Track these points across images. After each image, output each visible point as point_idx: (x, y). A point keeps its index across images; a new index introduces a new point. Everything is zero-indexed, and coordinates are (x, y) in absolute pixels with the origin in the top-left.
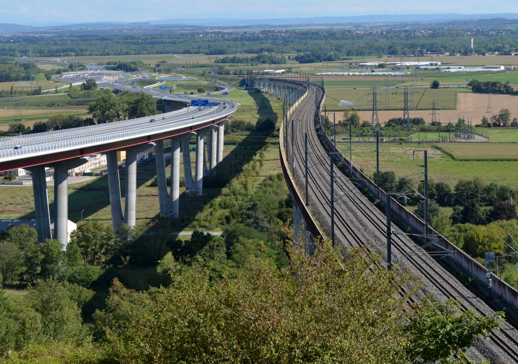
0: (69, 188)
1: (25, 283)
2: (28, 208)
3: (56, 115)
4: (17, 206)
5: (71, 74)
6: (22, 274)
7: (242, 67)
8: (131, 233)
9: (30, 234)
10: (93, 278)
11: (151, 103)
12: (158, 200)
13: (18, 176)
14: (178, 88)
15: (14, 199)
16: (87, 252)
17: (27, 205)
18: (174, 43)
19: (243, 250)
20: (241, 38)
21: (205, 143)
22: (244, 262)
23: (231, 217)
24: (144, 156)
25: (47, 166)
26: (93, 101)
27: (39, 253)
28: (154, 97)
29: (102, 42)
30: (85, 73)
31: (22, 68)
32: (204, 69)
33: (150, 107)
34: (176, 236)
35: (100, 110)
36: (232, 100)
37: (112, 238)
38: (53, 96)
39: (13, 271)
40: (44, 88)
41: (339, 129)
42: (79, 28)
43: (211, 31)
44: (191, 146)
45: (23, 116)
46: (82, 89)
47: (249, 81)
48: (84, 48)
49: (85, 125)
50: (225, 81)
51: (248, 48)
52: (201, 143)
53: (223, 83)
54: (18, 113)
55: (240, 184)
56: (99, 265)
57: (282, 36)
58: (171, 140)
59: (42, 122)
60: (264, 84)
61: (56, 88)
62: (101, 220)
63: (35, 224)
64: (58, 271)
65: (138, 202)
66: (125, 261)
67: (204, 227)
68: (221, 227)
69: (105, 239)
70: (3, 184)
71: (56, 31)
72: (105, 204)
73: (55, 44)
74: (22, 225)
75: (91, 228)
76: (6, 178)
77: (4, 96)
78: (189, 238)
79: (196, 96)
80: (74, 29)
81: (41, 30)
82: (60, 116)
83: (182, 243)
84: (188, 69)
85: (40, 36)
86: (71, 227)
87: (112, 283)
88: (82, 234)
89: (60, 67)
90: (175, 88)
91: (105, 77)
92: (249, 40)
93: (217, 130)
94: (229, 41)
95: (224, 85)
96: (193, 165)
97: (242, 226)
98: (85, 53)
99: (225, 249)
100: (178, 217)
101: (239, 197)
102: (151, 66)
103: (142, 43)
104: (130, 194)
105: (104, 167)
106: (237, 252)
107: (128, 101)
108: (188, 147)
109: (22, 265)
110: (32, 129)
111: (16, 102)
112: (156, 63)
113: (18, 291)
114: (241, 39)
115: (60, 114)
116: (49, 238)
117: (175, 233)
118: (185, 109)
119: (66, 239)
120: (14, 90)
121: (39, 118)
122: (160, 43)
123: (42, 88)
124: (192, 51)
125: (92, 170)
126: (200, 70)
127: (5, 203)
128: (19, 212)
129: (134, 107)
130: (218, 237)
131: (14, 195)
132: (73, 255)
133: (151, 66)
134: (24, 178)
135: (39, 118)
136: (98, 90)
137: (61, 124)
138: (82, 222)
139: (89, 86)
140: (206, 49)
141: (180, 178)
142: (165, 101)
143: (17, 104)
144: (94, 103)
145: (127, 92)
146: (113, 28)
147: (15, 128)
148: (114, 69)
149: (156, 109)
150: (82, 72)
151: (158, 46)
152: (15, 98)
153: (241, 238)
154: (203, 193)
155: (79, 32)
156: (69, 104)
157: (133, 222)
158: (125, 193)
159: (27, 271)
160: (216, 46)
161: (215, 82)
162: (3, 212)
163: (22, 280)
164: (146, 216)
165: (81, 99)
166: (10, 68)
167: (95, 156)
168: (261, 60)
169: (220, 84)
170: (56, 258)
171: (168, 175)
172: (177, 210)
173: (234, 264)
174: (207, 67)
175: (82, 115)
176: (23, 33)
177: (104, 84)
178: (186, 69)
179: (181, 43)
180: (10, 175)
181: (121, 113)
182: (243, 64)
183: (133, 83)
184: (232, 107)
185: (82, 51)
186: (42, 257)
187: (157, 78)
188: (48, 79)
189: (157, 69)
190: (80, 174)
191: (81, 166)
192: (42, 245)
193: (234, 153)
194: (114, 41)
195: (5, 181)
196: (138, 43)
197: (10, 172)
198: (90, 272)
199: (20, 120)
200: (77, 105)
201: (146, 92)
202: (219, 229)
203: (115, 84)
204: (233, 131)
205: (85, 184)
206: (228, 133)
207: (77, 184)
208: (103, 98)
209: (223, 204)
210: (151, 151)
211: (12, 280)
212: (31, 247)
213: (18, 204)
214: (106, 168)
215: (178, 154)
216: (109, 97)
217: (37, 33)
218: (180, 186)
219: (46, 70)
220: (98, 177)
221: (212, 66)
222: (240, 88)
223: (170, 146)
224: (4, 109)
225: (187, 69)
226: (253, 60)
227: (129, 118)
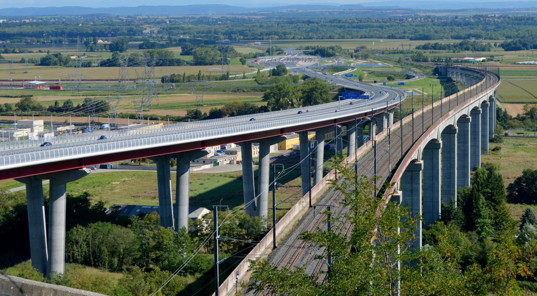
5: (267, 59)
7: (443, 54)
14: (370, 75)
18: (381, 27)
20: (451, 23)
29: (308, 25)
30: (280, 58)
38: (240, 82)
41: (516, 123)
42: (289, 10)
43: (424, 14)
47: (443, 70)
48: (288, 31)
50: (420, 69)
51: (456, 34)
53: (415, 70)
57: (494, 21)
60: (457, 73)
71: (266, 12)
73: (261, 26)
80: (285, 11)
81: (252, 12)
85: (249, 18)
92: (459, 25)
94: (438, 25)
95: (416, 73)
98: (288, 36)
103: (348, 27)
110: (208, 114)
111: (203, 87)
112: (355, 48)
114: (452, 24)
122: (367, 27)
124: (397, 36)
126: (397, 57)
133: (350, 51)
140: (412, 34)
146: (324, 11)
147: (193, 113)
148: (311, 54)
150: (278, 57)
151: (364, 30)
152: (201, 83)
155: (289, 14)
156: (254, 90)
160: (424, 30)
168: (464, 47)
176: (233, 14)
179: (389, 27)
182: (444, 51)
185: (285, 34)
189: (354, 54)
194: (320, 24)
196: (345, 26)
217: (246, 14)
221: (412, 52)
225: (385, 54)
226: (455, 46)
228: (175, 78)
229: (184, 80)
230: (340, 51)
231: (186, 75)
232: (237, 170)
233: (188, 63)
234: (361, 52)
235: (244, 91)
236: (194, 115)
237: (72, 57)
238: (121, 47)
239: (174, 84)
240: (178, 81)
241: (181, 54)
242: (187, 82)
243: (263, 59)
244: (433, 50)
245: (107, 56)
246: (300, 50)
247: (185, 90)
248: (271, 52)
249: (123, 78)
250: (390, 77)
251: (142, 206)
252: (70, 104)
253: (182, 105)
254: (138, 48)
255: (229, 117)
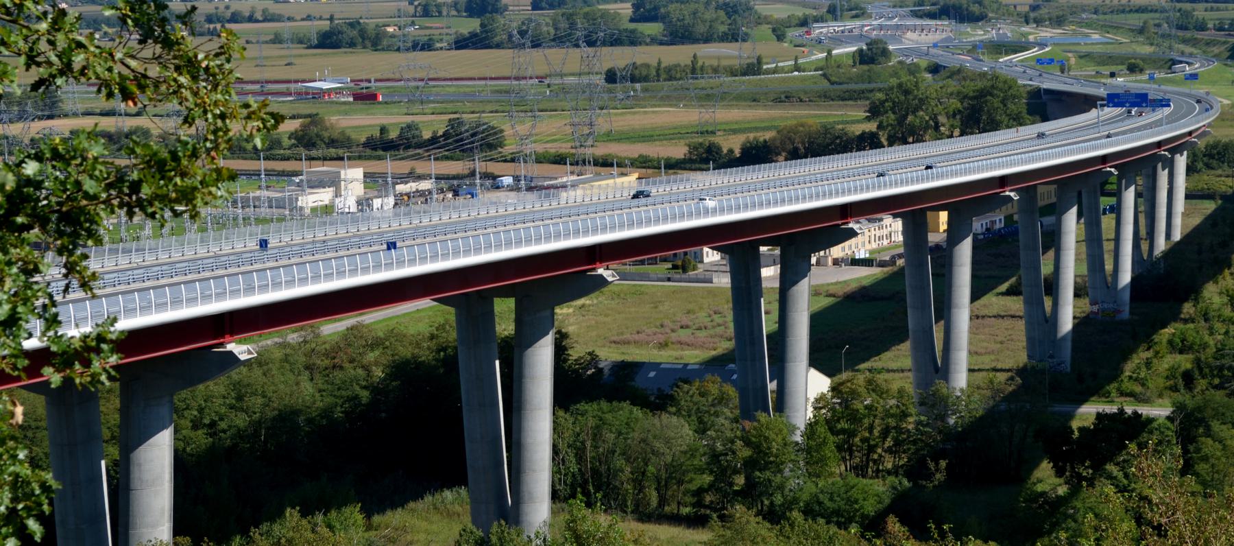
0: (815, 292)
1: (708, 512)
2: (721, 336)
3: (794, 122)
4: (699, 334)
6: (700, 492)
8: (954, 404)
9: (722, 400)
10: (862, 507)
11: (1014, 97)
12: (1023, 328)
13: (702, 262)
14: (1083, 61)
15: (692, 316)
16: (853, 445)
17: (720, 330)
19: (1219, 454)
21: (1138, 195)
22: (1222, 483)
23: (1197, 372)
24: (993, 223)
25: (765, 242)
26: (880, 90)
27: (739, 443)
28: (1020, 82)
30: (863, 26)
31: (722, 13)
32: (1145, 16)
33: (1011, 106)
34: (1071, 416)
35: (894, 113)
36: (1208, 93)
37: (911, 415)
39: (680, 482)
40: (769, 60)
44: (1105, 201)
45: (718, 124)
46: (854, 62)
49: (860, 148)
50: (1194, 45)
52: (1129, 196)
54: (707, 116)
55: (1221, 293)
56: (877, 477)
58: (1055, 186)
59: (761, 139)
61: (796, 59)
62: (888, 371)
63: (735, 377)
64: (781, 487)
65: (973, 331)
66: (937, 470)
67: (1131, 394)
68: (1171, 397)
69: (892, 416)
70: (669, 280)
72: (897, 335)
74: (709, 376)
75: (860, 390)
76: (675, 267)
77: (678, 76)
78: (1089, 422)
79: (1122, 82)
82: (802, 125)
83: (1072, 432)
84: (1107, 17)
86: (817, 384)
87: (885, 528)
88: (840, 404)
89: (808, 12)
90: (1073, 61)
91: (909, 35)
93: (1170, 165)
95: (1191, 55)
96: (1108, 246)
97: (1219, 396)
99: (1178, 450)
100: (1069, 370)
101: (1218, 326)
102: (1019, 8)
104: (955, 311)
105: (900, 246)
106: (1205, 459)
107: (959, 93)
108: (1097, 204)
109: (700, 471)
110: (737, 153)
111: (705, 92)
113: (691, 531)
115: (804, 120)
116: (766, 410)
117: (1058, 408)
118: (1094, 113)
119: (802, 413)
120: (700, 63)
121: (757, 129)
123: (764, 60)
125: (871, 252)
126: (1136, 20)
127: (671, 325)
128: (702, 347)
129: (973, 106)
130: (1161, 421)
131: (691, 306)
132: (817, 451)
133: (1019, 8)
134: (714, 268)
135: (757, 129)
136: (893, 66)
137: (803, 143)
138: (844, 376)
139: (872, 55)
141: (1076, 276)
142: (1048, 91)
143: (708, 95)
144: (880, 96)
145: (959, 71)
147: (701, 150)
149: (1025, 111)
150: (858, 23)
152: (702, 83)
153: (1216, 426)
154: (1131, 313)
156: (825, 97)
157: (960, 379)
158: (944, 309)
159: (711, 486)
161: (1170, 48)
162: (666, 345)
163: (699, 504)
164: (993, 365)
165: (852, 86)
166: (694, 14)
167: (881, 220)
169: (1183, 53)
170: (777, 457)
171: (1046, 269)
172: (1067, 352)
173: (1199, 488)
174: (1151, 11)
175: (853, 122)
177: (907, 52)
178: (1101, 17)
180: (684, 261)
181: (942, 119)
183: (974, 49)
184: (1207, 110)
186: (746, 453)
187: (1031, 38)
188: (780, 37)
189: (1032, 15)
190: (843, 260)
191: (847, 243)
192: (748, 424)
193: (1211, 221)
195: (673, 274)
197: (686, 254)
198: (854, 493)
199: (713, 133)
200: (843, 99)
201: (1004, 72)
202: (1167, 401)
203: (933, 51)
204: (1209, 167)
205: (854, 286)
206: (1198, 172)
207: (837, 283)
208: (900, 86)
209: (1178, 340)
210: (1010, 211)
211: (679, 503)
212: (723, 429)
213: (700, 329)
214: (901, 250)
215: (1071, 216)
216: (917, 83)
218: (1077, 295)
219: (775, 16)
220: (885, 269)
221: (1163, 11)
222: (1229, 62)
223: (1054, 200)
224: (676, 106)
227: (961, 135)
228: (637, 72)
229: (658, 75)
230: (998, 9)
231: (663, 65)
232: (841, 279)
233: (655, 41)
234: (1047, 11)
235: (801, 101)
236: (704, 155)
237: (390, 30)
238: (493, 5)
239: (638, 86)
240: (645, 79)
241: (632, 20)
242: (665, 80)
243: (822, 28)
244: (1213, 5)
245: (471, 25)
246: (901, 7)
247: (667, 100)
248: (839, 14)
249: (522, 74)
250: (1134, 64)
251: (660, 364)
252: (417, 133)
253: (666, 132)
254: (530, 8)
255: (786, 159)
